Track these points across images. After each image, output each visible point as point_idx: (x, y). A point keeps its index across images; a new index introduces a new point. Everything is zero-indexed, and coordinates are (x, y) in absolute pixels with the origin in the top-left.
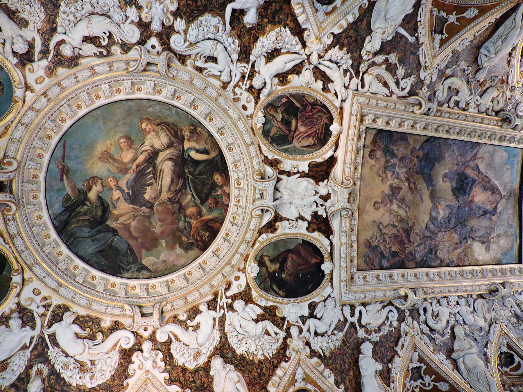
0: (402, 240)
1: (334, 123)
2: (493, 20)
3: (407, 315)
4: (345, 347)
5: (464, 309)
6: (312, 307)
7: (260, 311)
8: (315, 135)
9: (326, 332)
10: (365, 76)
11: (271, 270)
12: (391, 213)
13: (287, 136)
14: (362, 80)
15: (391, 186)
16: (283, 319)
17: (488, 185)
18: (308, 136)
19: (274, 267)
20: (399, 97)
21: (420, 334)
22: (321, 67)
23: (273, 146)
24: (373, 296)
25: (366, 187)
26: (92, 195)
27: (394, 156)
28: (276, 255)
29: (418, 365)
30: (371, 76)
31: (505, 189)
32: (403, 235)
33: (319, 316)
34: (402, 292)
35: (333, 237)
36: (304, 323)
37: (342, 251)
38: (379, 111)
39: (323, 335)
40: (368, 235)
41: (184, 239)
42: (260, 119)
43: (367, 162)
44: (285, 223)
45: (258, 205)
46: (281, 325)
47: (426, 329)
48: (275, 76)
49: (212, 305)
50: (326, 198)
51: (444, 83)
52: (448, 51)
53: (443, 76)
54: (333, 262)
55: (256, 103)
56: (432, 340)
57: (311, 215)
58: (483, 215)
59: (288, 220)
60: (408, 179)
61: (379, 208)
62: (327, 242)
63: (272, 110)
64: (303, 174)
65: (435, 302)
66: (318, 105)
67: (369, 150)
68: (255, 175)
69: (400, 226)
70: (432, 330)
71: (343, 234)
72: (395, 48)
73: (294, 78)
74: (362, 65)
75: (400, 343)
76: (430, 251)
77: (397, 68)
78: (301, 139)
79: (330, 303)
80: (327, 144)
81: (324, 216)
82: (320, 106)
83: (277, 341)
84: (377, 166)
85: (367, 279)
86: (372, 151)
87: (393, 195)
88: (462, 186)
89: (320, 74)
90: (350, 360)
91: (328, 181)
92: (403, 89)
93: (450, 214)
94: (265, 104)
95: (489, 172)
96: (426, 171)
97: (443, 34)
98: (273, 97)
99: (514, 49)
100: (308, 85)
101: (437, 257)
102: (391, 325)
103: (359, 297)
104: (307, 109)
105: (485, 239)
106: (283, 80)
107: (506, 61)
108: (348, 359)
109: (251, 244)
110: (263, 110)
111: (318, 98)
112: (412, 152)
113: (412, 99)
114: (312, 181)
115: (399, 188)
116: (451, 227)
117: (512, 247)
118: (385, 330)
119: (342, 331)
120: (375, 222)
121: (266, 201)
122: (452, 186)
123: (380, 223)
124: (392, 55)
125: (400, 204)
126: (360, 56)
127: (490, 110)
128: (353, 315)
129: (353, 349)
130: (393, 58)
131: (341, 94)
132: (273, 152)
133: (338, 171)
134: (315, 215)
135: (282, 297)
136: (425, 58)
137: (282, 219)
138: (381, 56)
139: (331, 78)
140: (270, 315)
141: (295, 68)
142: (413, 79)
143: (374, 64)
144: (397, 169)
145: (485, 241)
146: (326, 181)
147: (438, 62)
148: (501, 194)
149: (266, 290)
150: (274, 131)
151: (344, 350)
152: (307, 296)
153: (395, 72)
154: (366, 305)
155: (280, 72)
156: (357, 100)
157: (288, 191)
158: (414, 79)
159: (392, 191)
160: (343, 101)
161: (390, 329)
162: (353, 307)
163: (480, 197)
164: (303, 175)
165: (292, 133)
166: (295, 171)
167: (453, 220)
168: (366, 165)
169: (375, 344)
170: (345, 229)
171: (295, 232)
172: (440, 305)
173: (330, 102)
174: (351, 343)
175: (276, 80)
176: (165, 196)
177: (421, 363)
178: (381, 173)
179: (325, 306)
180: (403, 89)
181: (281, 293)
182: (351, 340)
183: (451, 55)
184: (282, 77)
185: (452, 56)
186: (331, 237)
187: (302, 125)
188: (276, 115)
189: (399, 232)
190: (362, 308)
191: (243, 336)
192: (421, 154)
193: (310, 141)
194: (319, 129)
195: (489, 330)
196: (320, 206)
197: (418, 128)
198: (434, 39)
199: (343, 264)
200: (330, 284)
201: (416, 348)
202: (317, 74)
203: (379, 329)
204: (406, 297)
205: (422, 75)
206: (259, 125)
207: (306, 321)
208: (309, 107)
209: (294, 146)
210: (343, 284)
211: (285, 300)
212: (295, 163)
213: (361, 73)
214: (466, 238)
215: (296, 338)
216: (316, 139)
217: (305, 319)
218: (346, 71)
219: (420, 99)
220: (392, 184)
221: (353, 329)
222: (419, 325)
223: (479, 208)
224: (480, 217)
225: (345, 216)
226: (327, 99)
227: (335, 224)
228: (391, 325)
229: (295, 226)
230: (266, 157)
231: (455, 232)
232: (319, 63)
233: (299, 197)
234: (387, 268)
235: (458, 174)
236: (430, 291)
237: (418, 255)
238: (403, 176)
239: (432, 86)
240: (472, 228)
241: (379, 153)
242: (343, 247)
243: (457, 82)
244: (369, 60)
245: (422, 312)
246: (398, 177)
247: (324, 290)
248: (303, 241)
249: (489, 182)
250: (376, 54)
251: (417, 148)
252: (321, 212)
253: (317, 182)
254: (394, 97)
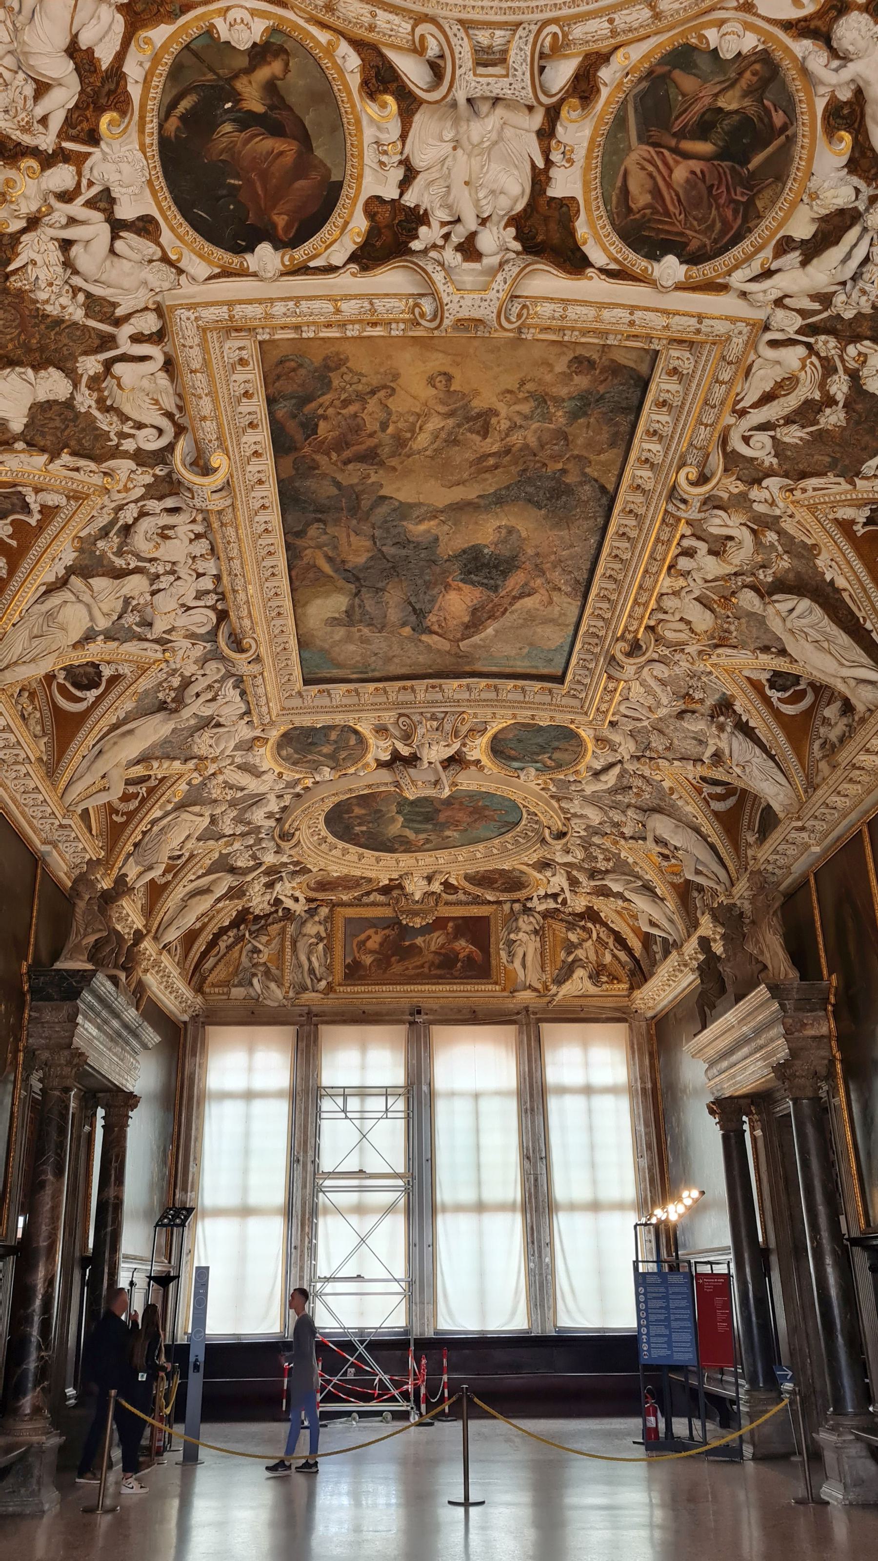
0: (348, 445)
1: (684, 267)
2: (868, 626)
3: (157, 471)
4: (43, 327)
5: (188, 588)
6: (145, 227)
7: (105, 56)
8: (655, 212)
9: (76, 272)
10: (801, 351)
11: (241, 85)
12: (419, 416)
13: (666, 126)
14: (791, 342)
15: (492, 412)
16: (93, 138)
17: (485, 615)
18: (656, 193)
20: (728, 428)
21: (113, 505)
22: (855, 231)
23: (641, 79)
24: (199, 391)
25: (492, 352)
27: (574, 416)
28: (292, 99)
29: (35, 507)
30: (797, 364)
31: (475, 646)
32: (363, 447)
33: (119, 245)
34: (217, 460)
35: (353, 275)
36: (90, 204)
37: (316, 305)
38: (699, 385)
39: (68, 264)
40: (361, 362)
42: (734, 40)
43: (564, 353)
44: (394, 129)
45: (457, 49)
46: (73, 132)
47: (128, 515)
48: (859, 93)
50: (469, 249)
51: (744, 528)
52: (818, 536)
53: (761, 524)
54: (283, 274)
55: (787, 26)
56: (104, 532)
57: (417, 206)
58: (414, 609)
59: (404, 137)
60: (508, 451)
61: (434, 386)
62: (338, 256)
63: (755, 79)
64: (543, 178)
65: (199, 528)
66: (745, 220)
67: (595, 357)
68: (554, 28)
69: (386, 437)
70: (127, 529)
71: (366, 304)
72: (858, 423)
73: (839, 154)
74: (832, 342)
75: (82, 463)
76: (321, 509)
77: (803, 427)
78: (651, 168)
79: (159, 277)
80: (627, 251)
81: (416, 245)
82: (740, 227)
83: (26, 129)
84: (548, 378)
85: (239, 368)
86: (591, 364)
88: (485, 568)
89: (834, 227)
90: (10, 346)
91: (518, 253)
92: (746, 440)
93: (417, 546)
94: (778, 54)
95: (515, 616)
96: (530, 490)
97: (865, 525)
98: (796, 85)
99: (794, 661)
100: (810, 195)
101: (308, 524)
102: (122, 435)
103: (191, 356)
104: (739, 189)
105: (357, 617)
106: (843, 118)
107: (767, 643)
108: (12, 340)
109: (327, 18)
110: (760, 48)
111: (764, 223)
113: (717, 461)
114: (520, 206)
115: (485, 432)
116: (384, 549)
117: (339, 666)
118: (104, 422)
119: (87, 315)
120: (396, 377)
121: (470, 76)
122: (486, 546)
123: (393, 390)
124: (842, 415)
125: (443, 435)
126: (856, 338)
127: (662, 616)
128: (136, 339)
129: (42, 349)
130: (833, 419)
131: (765, 292)
132: (621, 84)
133: (547, 282)
134: (417, 218)
135: (161, 126)
136: (815, 489)
137: (407, 114)
138: (845, 389)
139: (815, 261)
140: (97, 93)
141: (869, 154)
142: (770, 461)
143: (828, 368)
144: (535, 426)
145: (350, 618)
146: (517, 246)
147: (798, 516)
148: (463, 639)
149: (176, 71)
150: (687, 82)
151: (36, 325)
152: (174, 208)
153: (794, 422)
154: (167, 371)
155: (869, 110)
156: (740, 333)
157: (494, 136)
158: (767, 464)
159: (479, 415)
160: (744, 294)
161: (112, 435)
162: (158, 337)
163: (457, 602)
164: (540, 179)
165: (673, 143)
166: (555, 157)
167: (404, 552)
168: (555, 350)
169: (69, 404)
170: (380, 309)
171: (367, 161)
172: (191, 541)
173: (749, 258)
174: (56, 341)
175: (845, 95)
177: (40, 512)
178: (530, 386)
179: (151, 261)
180: (746, 440)
181: (173, 123)
182: (66, 341)
183: (809, 542)
184: (853, 112)
185: (805, 544)
186: (354, 267)
187: (693, 173)
188: (737, 92)
189: (371, 435)
190: (160, 359)
191: (17, 8)
192: (571, 479)
193: (641, 198)
194: (672, 224)
195: (147, 640)
196: (445, 230)
197: (639, 473)
198: (859, 507)
199: (279, 309)
200: (217, 270)
201: (76, 498)
202: (837, 220)
203: (106, 409)
204: (207, 470)
205: (773, 483)
206: (712, 36)
207: (98, 209)
208: (743, 194)
209: (630, 149)
210: (223, 312)
211: (152, 140)
212: (580, 155)
213: (812, 340)
214: (358, 579)
215: (44, 186)
216: (644, 216)
217: (102, 205)
218: (825, 299)
219: (714, 482)
221: (97, 342)
222: (136, 501)
223: (433, 601)
224: (410, 603)
225: (417, 310)
226: (759, 249)
227: (391, 279)
228: (122, 435)
229: (384, 159)
230: (604, 58)
231: (372, 558)
232: (865, 230)
233: (471, 167)
234: (271, 413)
235: (514, 558)
236: (226, 519)
237: (310, 483)
238: (516, 439)
239: (742, 502)
240: (383, 590)
241: (582, 382)
242: (329, 307)
243: (743, 553)
244: (843, 360)
245: (170, 503)
246: (514, 427)
247: (198, 259)
248: (339, 185)
249: (492, 616)
250: (854, 376)
251: (587, 470)
252: (427, 235)
253: (515, 221)
254: (732, 420)
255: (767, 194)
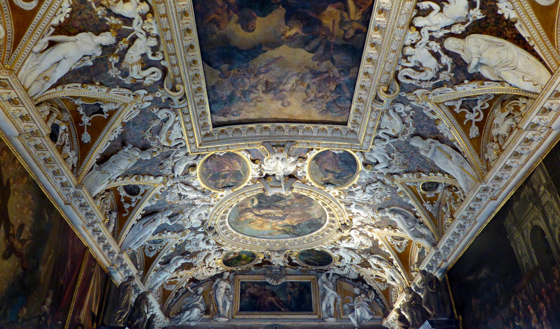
18: (232, 164)
19: (330, 177)
26: (280, 228)
41: (306, 205)
49: (348, 205)
56: (440, 85)
84: (246, 108)
87: (275, 89)
112: (225, 78)
136: (131, 111)
143: (159, 143)
147: (126, 97)
158: (154, 109)
176: (280, 211)
218: (174, 158)
220: (263, 92)
228: (408, 113)
238: (253, 81)
239: (151, 89)
246: (255, 87)
254: (177, 119)
255: (204, 171)
